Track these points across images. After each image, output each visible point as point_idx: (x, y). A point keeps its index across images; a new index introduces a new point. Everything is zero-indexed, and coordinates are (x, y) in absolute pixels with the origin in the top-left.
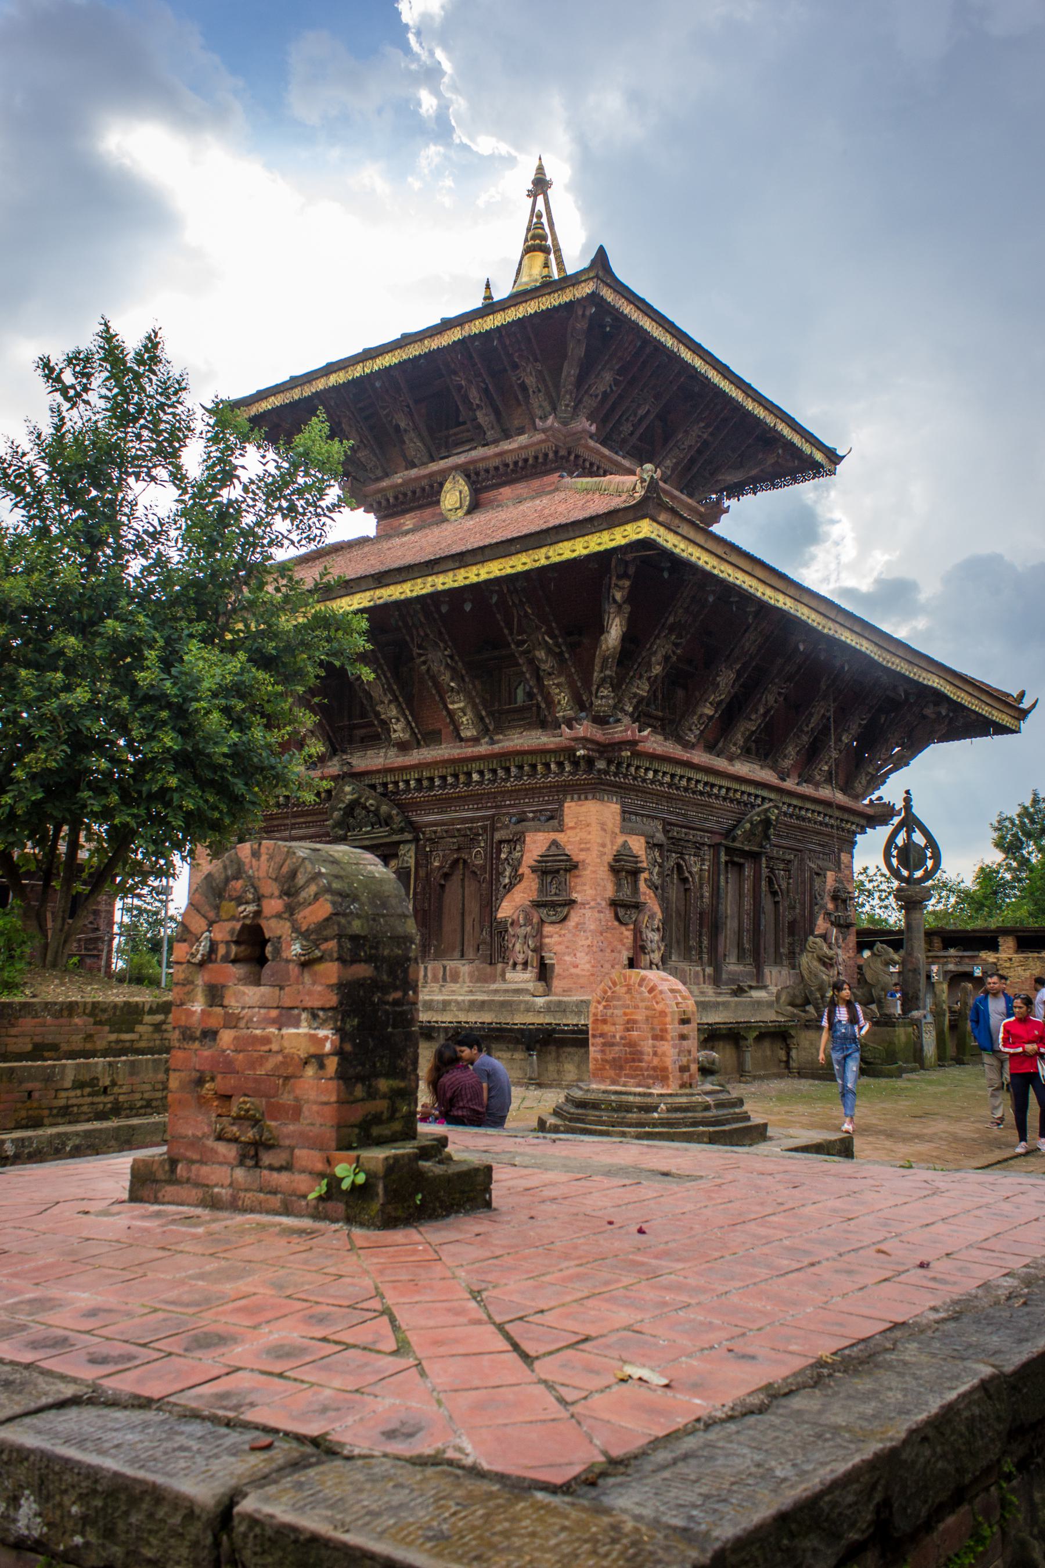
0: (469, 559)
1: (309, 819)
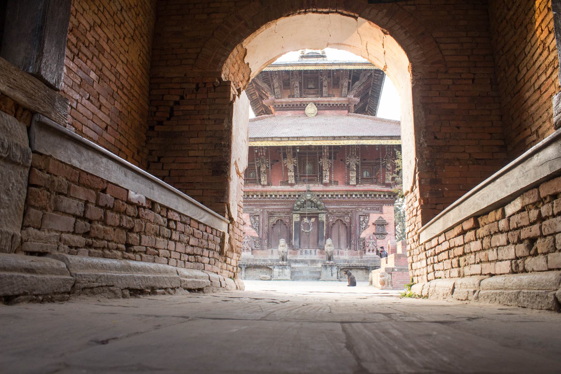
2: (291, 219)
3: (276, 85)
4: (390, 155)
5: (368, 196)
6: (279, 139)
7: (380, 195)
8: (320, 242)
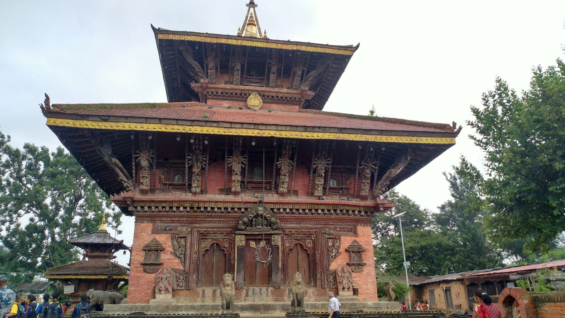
0: (384, 133)
1: (221, 220)
2: (232, 242)
3: (211, 65)
4: (370, 158)
5: (338, 212)
6: (229, 125)
7: (354, 211)
8: (273, 276)
